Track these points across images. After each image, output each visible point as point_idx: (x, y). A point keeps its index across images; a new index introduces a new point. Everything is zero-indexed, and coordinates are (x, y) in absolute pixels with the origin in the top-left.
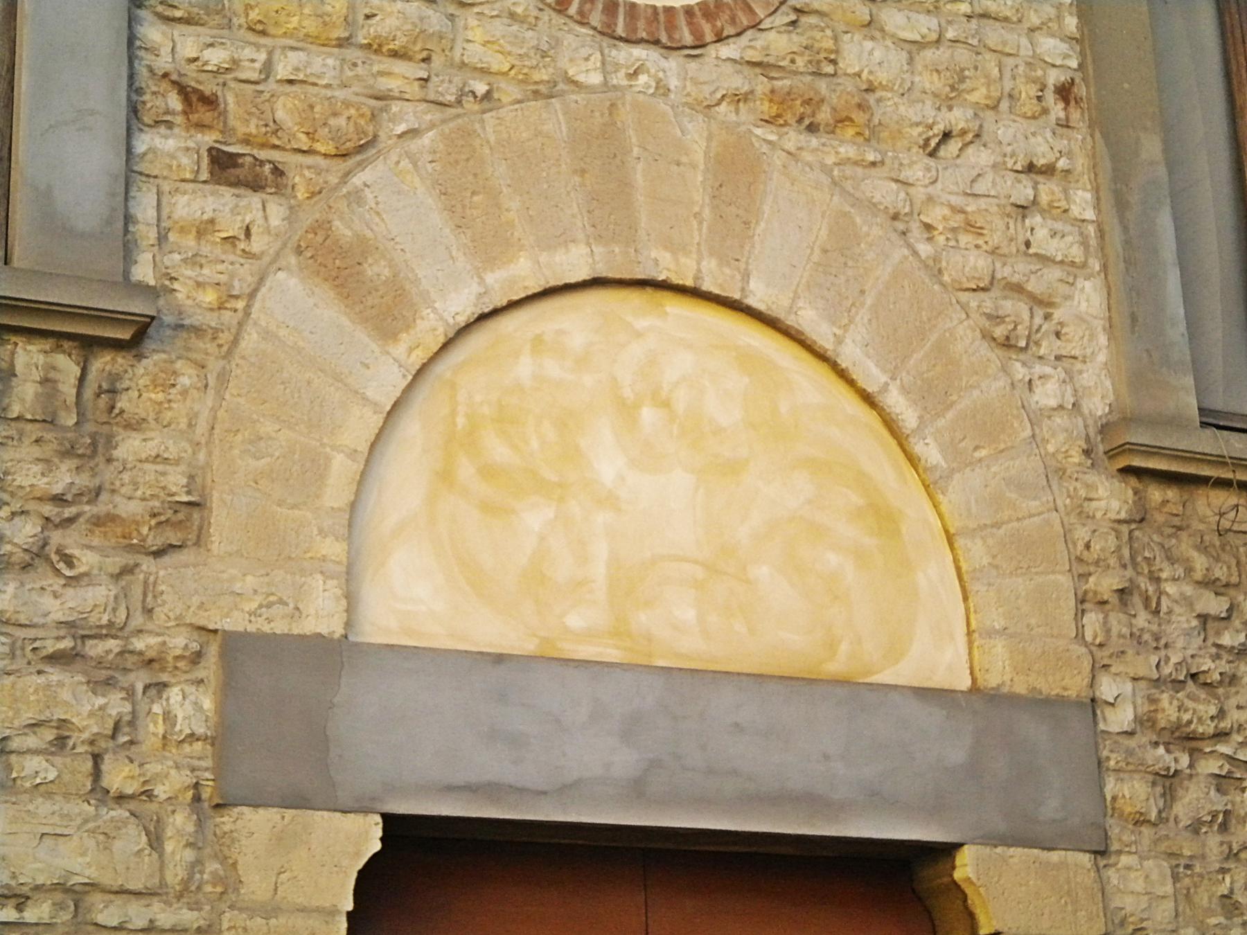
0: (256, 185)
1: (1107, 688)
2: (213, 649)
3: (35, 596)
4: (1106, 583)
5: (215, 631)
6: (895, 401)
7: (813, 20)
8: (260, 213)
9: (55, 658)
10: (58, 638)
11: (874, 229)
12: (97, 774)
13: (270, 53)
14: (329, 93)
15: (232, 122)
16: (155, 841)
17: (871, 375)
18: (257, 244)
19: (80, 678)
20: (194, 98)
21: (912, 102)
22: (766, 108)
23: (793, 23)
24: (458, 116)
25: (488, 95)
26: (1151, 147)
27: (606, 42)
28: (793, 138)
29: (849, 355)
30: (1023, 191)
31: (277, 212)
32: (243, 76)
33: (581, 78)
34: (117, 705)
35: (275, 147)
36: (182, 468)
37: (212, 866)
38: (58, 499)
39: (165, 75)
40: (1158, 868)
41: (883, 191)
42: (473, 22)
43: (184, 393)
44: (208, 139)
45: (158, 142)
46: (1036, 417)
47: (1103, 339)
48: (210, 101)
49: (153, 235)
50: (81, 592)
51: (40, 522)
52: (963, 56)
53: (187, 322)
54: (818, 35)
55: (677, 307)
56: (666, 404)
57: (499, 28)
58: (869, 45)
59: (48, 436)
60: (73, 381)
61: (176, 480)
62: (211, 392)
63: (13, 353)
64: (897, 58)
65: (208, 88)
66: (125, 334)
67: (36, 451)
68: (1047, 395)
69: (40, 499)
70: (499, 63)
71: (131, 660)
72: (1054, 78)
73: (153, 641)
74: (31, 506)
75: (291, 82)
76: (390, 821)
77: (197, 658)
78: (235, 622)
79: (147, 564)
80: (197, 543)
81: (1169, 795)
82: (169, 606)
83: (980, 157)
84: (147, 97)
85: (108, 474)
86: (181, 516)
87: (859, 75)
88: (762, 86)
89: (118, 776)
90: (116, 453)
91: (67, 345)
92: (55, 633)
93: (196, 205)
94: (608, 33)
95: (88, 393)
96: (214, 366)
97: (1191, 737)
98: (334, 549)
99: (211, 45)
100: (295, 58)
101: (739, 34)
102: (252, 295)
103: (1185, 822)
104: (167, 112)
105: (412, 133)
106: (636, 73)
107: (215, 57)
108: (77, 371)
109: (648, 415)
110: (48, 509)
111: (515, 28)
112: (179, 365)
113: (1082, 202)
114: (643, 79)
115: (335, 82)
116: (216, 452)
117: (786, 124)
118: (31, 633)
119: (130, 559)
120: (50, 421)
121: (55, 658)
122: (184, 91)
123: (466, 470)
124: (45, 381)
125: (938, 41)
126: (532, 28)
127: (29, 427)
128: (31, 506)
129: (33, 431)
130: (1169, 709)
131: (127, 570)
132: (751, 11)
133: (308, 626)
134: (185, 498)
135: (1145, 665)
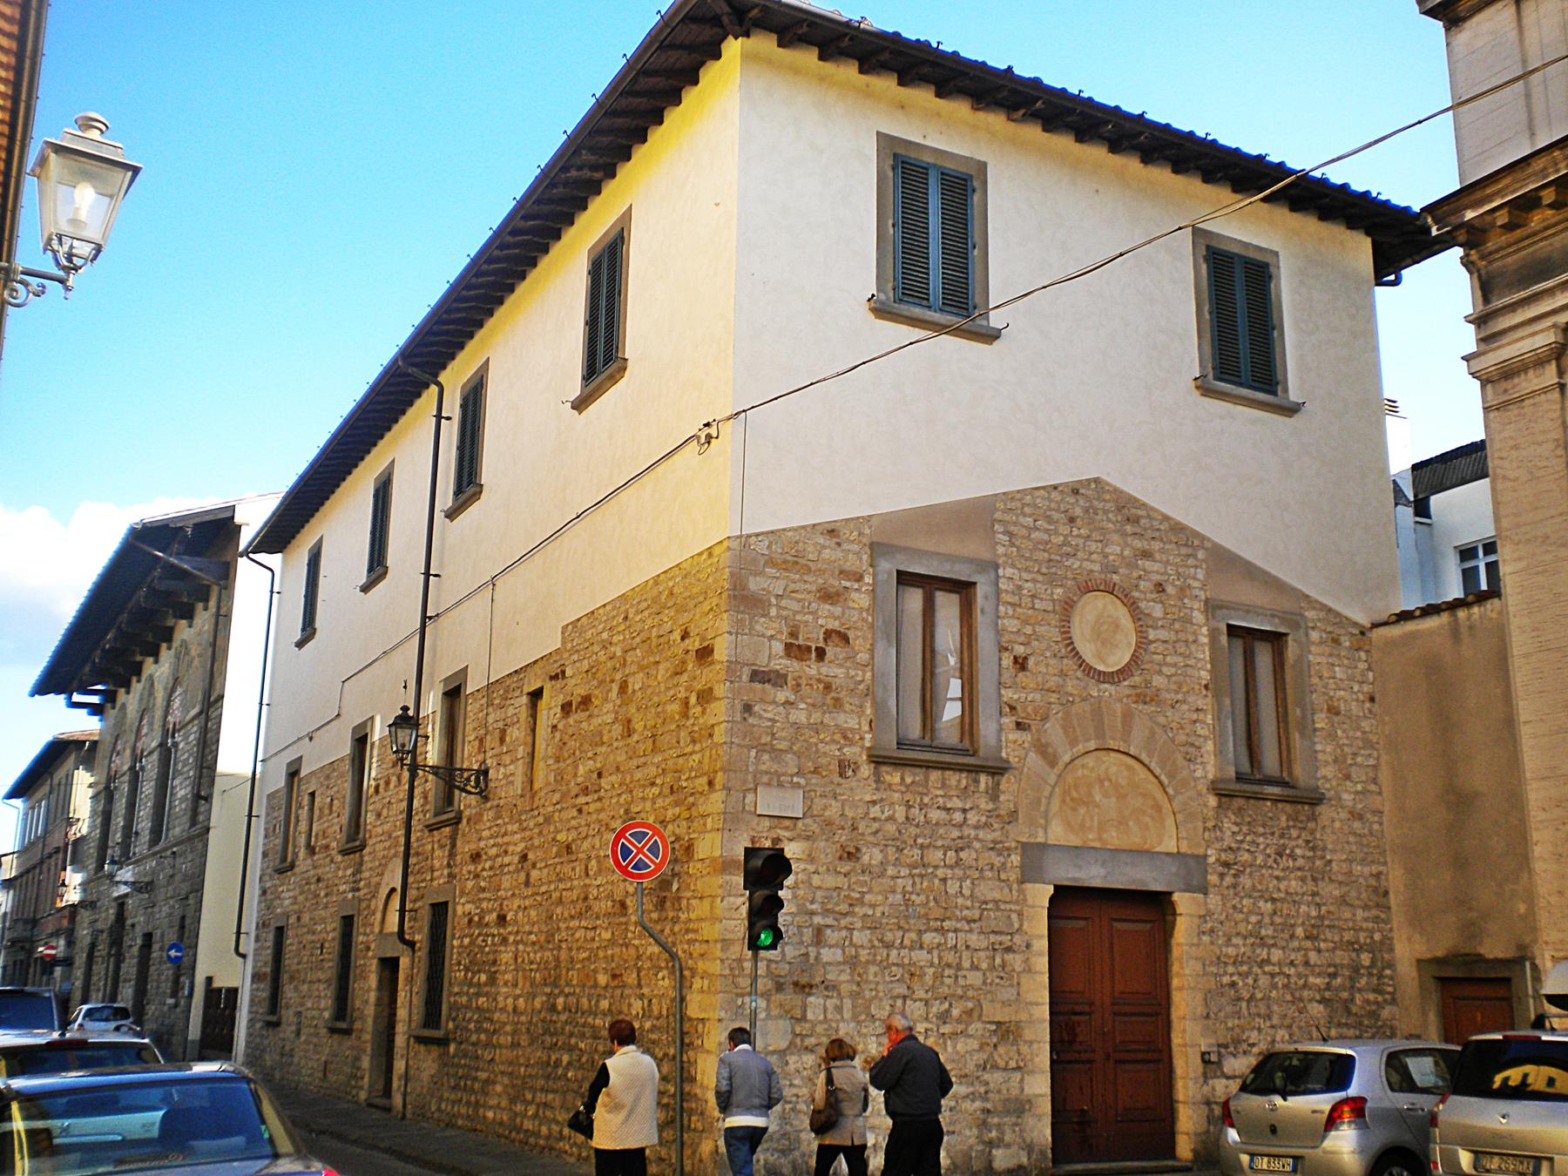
0: (1024, 730)
1: (1209, 852)
4: (1210, 824)
6: (1163, 778)
9: (992, 849)
11: (1159, 731)
17: (1158, 771)
18: (1026, 745)
26: (1227, 702)
29: (1153, 766)
30: (1195, 716)
34: (1002, 860)
40: (1219, 898)
41: (1162, 720)
44: (1014, 718)
46: (1196, 779)
52: (1182, 678)
55: (1113, 754)
56: (1110, 780)
57: (1075, 682)
61: (1012, 806)
68: (1199, 774)
70: (1075, 692)
72: (1204, 682)
78: (1024, 840)
81: (1222, 879)
82: (1012, 836)
83: (1185, 707)
88: (1133, 692)
94: (1099, 681)
98: (1042, 821)
107: (1016, 697)
109: (1106, 784)
120: (987, 792)
121: (992, 849)
123: (1068, 799)
130: (1223, 857)
135: (1218, 845)
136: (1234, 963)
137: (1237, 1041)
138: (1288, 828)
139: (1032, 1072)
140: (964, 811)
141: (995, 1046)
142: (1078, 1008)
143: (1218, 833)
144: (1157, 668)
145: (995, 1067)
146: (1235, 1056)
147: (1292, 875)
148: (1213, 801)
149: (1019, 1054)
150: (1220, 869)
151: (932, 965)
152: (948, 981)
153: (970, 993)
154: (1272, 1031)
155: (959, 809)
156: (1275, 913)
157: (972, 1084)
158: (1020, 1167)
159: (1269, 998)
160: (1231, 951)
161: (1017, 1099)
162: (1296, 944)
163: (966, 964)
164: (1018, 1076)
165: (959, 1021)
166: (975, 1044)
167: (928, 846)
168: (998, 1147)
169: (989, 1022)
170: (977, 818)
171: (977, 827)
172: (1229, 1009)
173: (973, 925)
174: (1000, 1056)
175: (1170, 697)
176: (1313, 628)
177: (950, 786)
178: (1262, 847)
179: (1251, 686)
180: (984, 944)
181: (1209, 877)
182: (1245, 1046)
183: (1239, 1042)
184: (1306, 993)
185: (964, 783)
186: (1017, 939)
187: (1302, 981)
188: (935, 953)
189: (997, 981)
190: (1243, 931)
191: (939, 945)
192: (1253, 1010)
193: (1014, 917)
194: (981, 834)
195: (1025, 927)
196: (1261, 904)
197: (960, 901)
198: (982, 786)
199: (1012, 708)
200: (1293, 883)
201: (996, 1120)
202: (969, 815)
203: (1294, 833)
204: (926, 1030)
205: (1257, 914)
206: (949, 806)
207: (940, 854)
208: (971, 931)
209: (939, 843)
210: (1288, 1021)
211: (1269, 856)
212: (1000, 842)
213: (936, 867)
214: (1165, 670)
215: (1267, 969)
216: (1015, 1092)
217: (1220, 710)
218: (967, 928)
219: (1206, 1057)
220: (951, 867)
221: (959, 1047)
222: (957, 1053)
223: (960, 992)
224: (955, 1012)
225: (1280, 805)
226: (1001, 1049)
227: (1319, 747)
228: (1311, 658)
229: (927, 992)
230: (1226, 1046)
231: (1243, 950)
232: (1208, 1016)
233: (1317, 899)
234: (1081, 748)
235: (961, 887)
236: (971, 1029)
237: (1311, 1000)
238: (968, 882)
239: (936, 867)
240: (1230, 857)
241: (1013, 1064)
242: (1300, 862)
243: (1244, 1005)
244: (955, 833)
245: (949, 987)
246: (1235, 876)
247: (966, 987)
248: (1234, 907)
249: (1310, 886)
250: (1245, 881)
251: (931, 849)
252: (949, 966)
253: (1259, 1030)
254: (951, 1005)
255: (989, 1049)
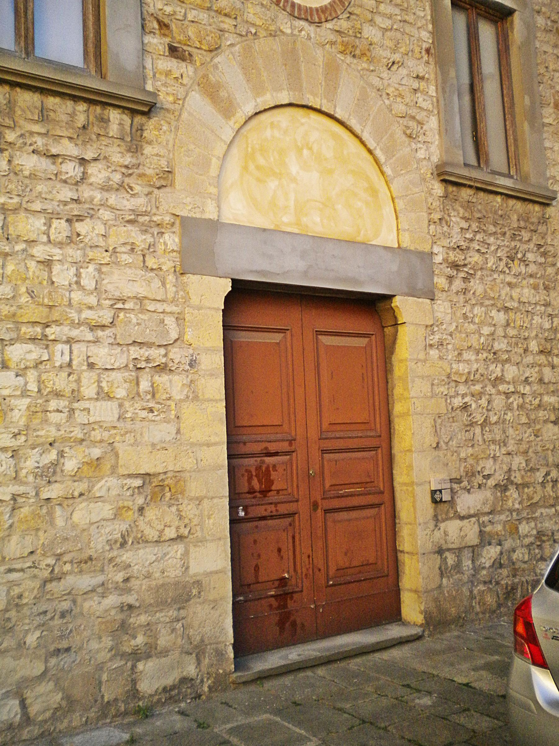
0: (183, 59)
1: (436, 249)
2: (178, 222)
3: (121, 200)
4: (436, 216)
5: (178, 216)
6: (378, 153)
7: (354, 17)
8: (185, 70)
9: (129, 222)
10: (131, 215)
11: (373, 94)
12: (144, 262)
13: (186, 10)
14: (205, 27)
15: (174, 35)
16: (164, 284)
17: (372, 144)
18: (185, 81)
19: (137, 229)
20: (162, 24)
21: (384, 50)
22: (341, 48)
23: (348, 17)
24: (246, 40)
25: (256, 33)
27: (292, 18)
28: (349, 59)
29: (365, 136)
30: (416, 85)
31: (191, 69)
32: (177, 17)
33: (284, 30)
34: (150, 239)
35: (188, 45)
36: (165, 159)
37: (181, 293)
38: (127, 167)
39: (152, 14)
40: (447, 304)
41: (376, 81)
42: (250, 5)
43: (165, 132)
44: (167, 40)
45: (151, 40)
47: (437, 137)
48: (167, 26)
49: (151, 74)
50: (136, 199)
51: (121, 174)
52: (399, 35)
53: (164, 107)
54: (356, 23)
55: (314, 116)
56: (310, 149)
57: (258, 9)
58: (371, 28)
59: (122, 144)
60: (129, 125)
61: (163, 163)
62: (173, 133)
63: (109, 113)
64: (379, 34)
65: (166, 21)
66: (146, 109)
67: (118, 149)
68: (421, 154)
69: (121, 166)
70: (259, 22)
71: (152, 224)
72: (425, 46)
73: (159, 218)
74: (118, 168)
75: (193, 22)
76: (234, 281)
77: (173, 224)
78: (184, 213)
79: (156, 191)
80: (171, 185)
81: (450, 283)
82: (164, 207)
83: (403, 72)
84: (146, 22)
85: (141, 159)
86: (165, 176)
87: (368, 38)
88: (339, 40)
89: (151, 262)
90: (144, 152)
91: (126, 111)
92: (128, 213)
93: (165, 64)
95: (134, 130)
96: (173, 123)
97: (457, 266)
99: (167, 5)
100: (194, 12)
101: (332, 20)
102: (185, 99)
103: (454, 291)
104: (154, 29)
105: (232, 45)
106: (301, 30)
108: (130, 121)
109: (305, 152)
110: (124, 170)
111: (263, 9)
112: (162, 122)
113: (432, 90)
114: (303, 33)
115: (207, 24)
116: (176, 154)
117: (346, 54)
118: (121, 213)
119: (151, 189)
120: (122, 139)
121: (129, 222)
122: (159, 22)
123: (251, 167)
124: (120, 124)
125: (391, 29)
126: (268, 10)
127: (115, 140)
128: (118, 168)
129: (118, 142)
130: (452, 256)
131: (149, 193)
132: (335, 11)
133: (207, 216)
134: (167, 170)
135: (446, 243)
136: (466, 381)
137: (471, 474)
138: (520, 228)
139: (202, 541)
140: (83, 161)
141: (141, 510)
142: (273, 447)
143: (445, 228)
144: (369, 16)
145: (141, 541)
146: (469, 491)
147: (525, 282)
148: (438, 189)
149: (181, 518)
150: (449, 271)
151: (24, 393)
152: (54, 417)
153: (97, 435)
154: (507, 459)
155: (71, 158)
156: (508, 325)
157: (102, 571)
158: (184, 680)
159: (504, 421)
160: (462, 368)
161: (177, 584)
162: (529, 359)
163: (89, 390)
164: (180, 548)
165: (76, 477)
166: (107, 511)
167: (15, 210)
168: (148, 656)
169: (130, 476)
170: (104, 174)
171: (106, 188)
172: (461, 436)
173: (100, 333)
174: (149, 523)
175: (384, 54)
176: (538, 12)
177: (56, 122)
178: (493, 248)
179: (474, 58)
180: (122, 361)
181: (436, 279)
182: (479, 479)
183: (473, 475)
184: (541, 413)
185: (81, 119)
186: (176, 354)
187: (537, 402)
188: (32, 375)
189: (144, 414)
190: (475, 345)
191: (38, 364)
192: (488, 436)
193: (170, 321)
194: (113, 199)
195: (188, 337)
196: (494, 313)
197: (76, 296)
198: (114, 129)
199: (163, 25)
200: (526, 291)
201: (143, 619)
202: (92, 169)
203: (526, 235)
204: (14, 498)
205: (490, 325)
206: (54, 151)
207: (39, 223)
208: (96, 341)
209: (37, 206)
210: (524, 446)
211: (501, 260)
212: (146, 213)
213: (31, 242)
214: (378, 20)
215: (502, 388)
216: (174, 573)
217: (444, 82)
218: (89, 336)
219: (437, 496)
220: (60, 245)
221: (76, 517)
222: (74, 526)
223: (78, 433)
224: (70, 465)
225: (511, 202)
226: (151, 513)
227: (547, 144)
228: (538, 44)
229: (15, 436)
230: (458, 481)
231: (475, 366)
232: (437, 447)
233: (550, 310)
234: (269, 100)
235: (78, 275)
236: (99, 489)
237: (545, 422)
238: (91, 268)
239: (31, 242)
240: (457, 257)
241: (171, 533)
242: (533, 268)
243: (478, 430)
244: (67, 194)
245: (58, 427)
246: (465, 279)
247: (89, 426)
248: (465, 316)
249: (542, 296)
250: (476, 286)
251: (22, 214)
252: (58, 395)
253: (495, 458)
254: (61, 454)
255: (131, 515)
